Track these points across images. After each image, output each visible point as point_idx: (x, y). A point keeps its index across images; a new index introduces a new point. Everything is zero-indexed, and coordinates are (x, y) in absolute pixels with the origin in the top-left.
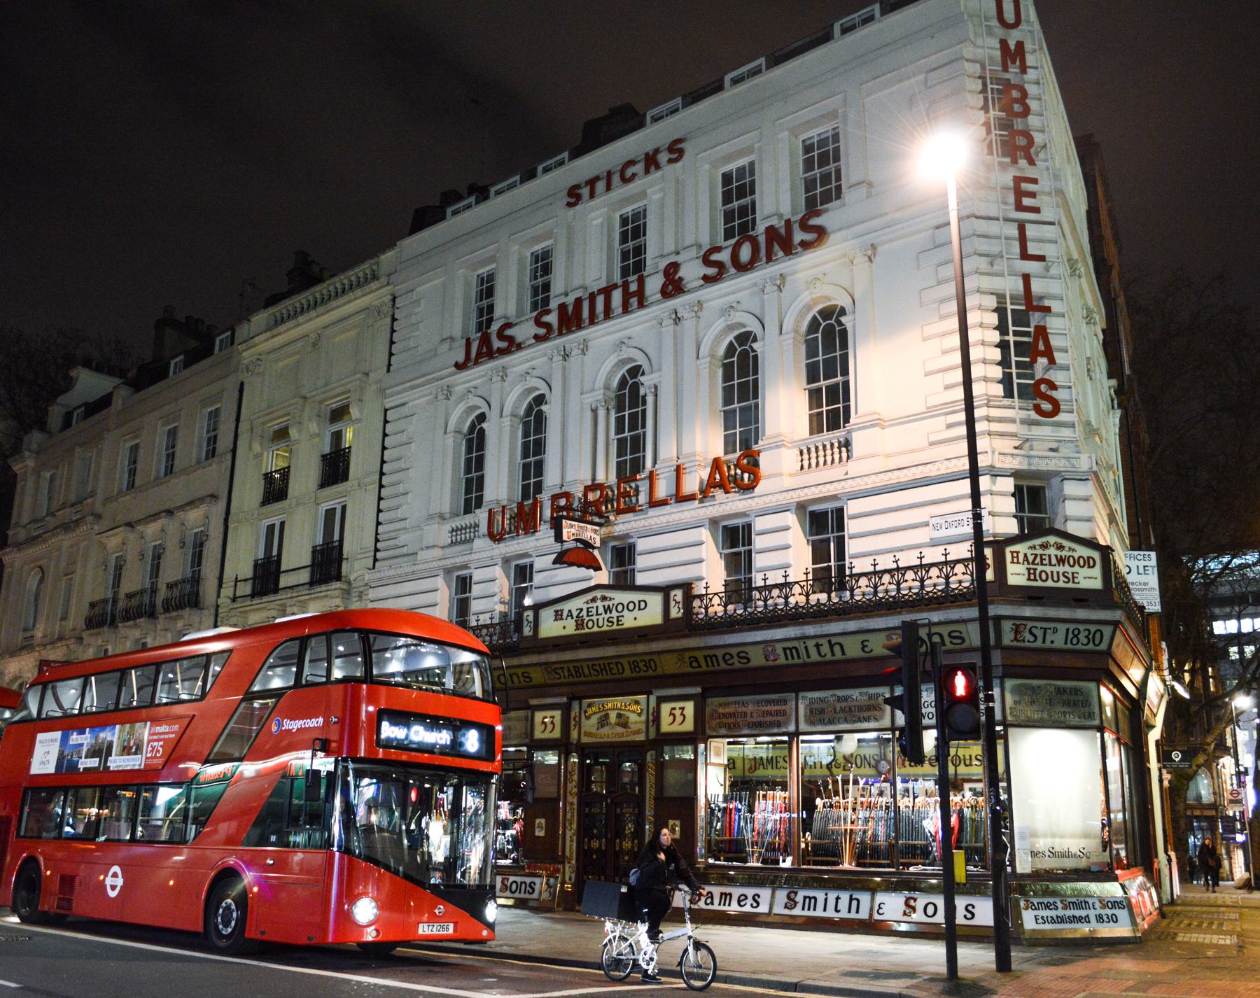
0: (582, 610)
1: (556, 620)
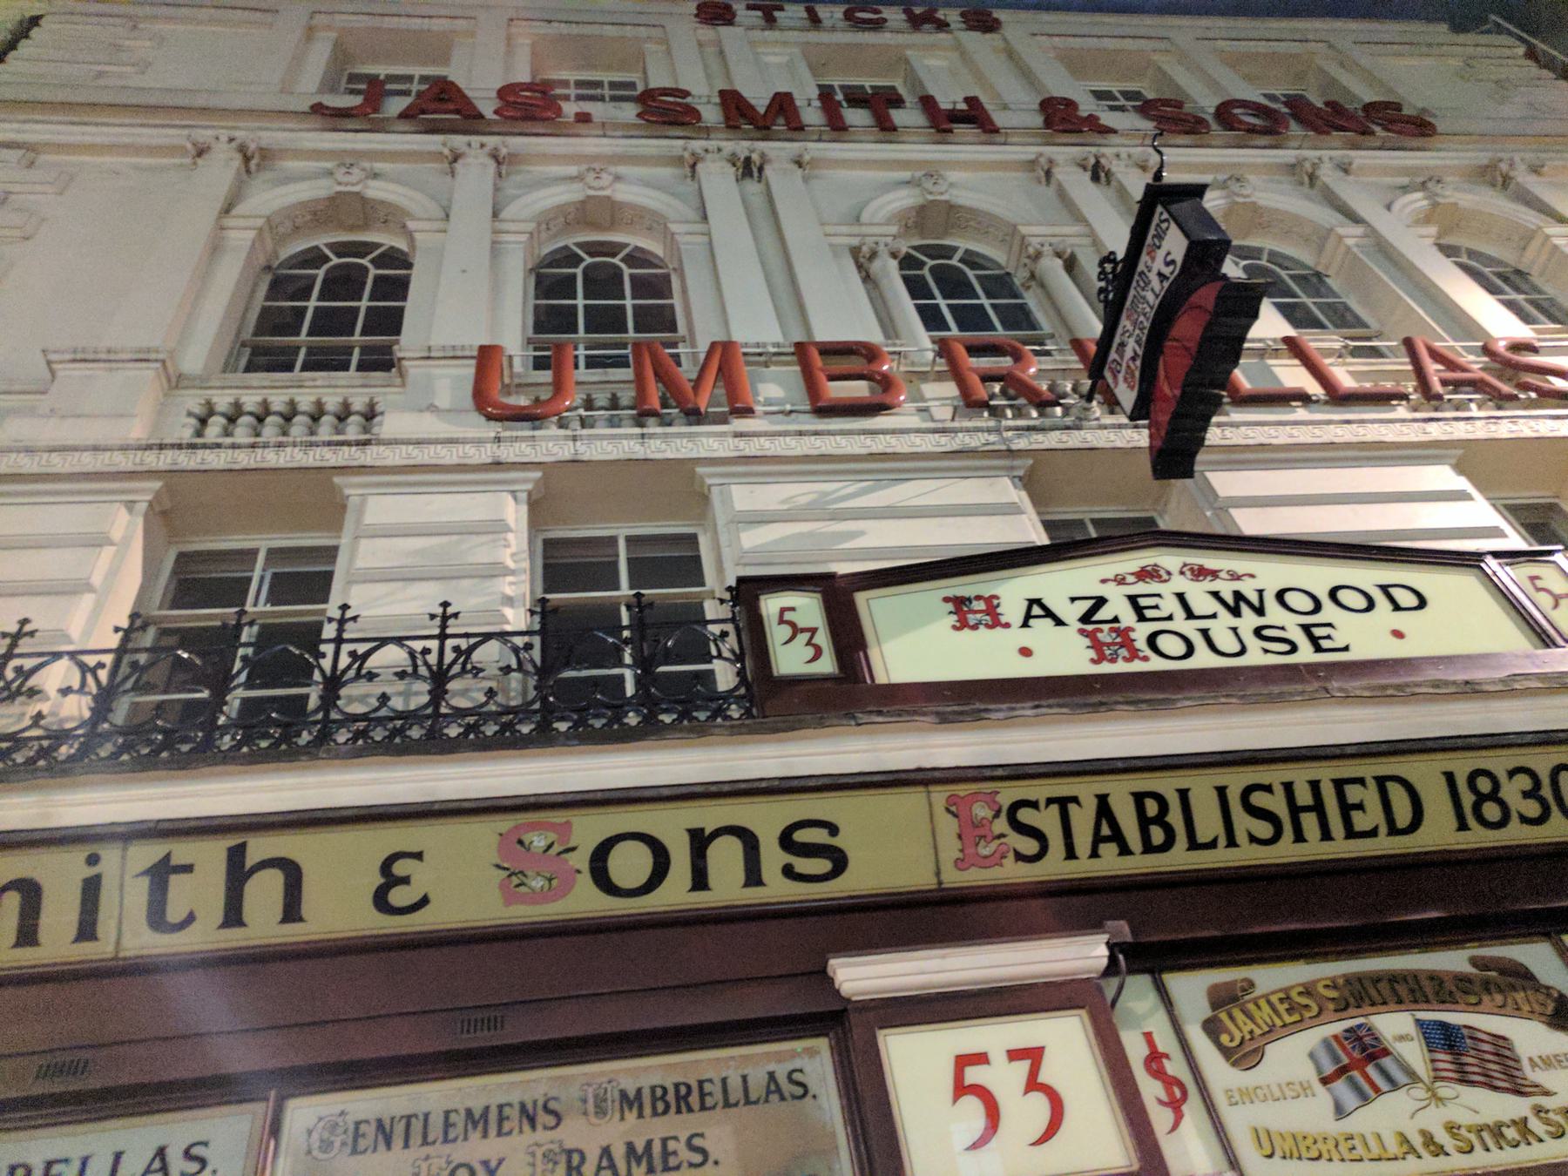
0: (1100, 602)
1: (962, 624)
